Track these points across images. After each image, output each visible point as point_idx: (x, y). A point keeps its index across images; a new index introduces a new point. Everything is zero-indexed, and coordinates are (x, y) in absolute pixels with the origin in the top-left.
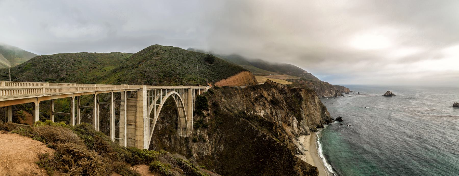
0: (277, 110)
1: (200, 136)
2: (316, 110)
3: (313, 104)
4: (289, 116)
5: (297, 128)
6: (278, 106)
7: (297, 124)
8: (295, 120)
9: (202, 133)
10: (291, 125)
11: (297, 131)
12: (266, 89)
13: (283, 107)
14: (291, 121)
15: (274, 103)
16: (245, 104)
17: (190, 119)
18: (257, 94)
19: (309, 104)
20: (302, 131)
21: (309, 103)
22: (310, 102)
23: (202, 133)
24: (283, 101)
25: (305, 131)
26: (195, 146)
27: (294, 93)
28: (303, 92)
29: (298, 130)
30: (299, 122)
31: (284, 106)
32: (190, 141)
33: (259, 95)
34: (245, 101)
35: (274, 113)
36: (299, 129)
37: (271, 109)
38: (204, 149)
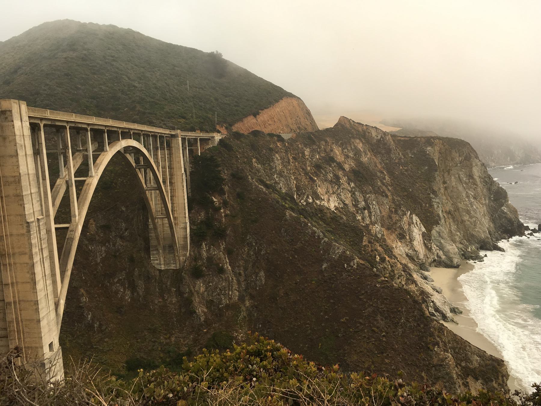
0: (368, 196)
1: (210, 259)
2: (475, 198)
3: (467, 181)
4: (400, 212)
5: (423, 247)
7: (424, 235)
9: (214, 252)
10: (408, 238)
11: (425, 255)
13: (384, 187)
14: (406, 227)
16: (293, 178)
17: (181, 220)
18: (319, 153)
19: (453, 181)
20: (438, 256)
21: (455, 178)
22: (457, 176)
23: (214, 252)
24: (382, 172)
26: (200, 286)
28: (437, 148)
30: (429, 229)
32: (187, 277)
33: (323, 157)
34: (291, 172)
35: (362, 204)
36: (429, 249)
37: (354, 194)
38: (220, 289)
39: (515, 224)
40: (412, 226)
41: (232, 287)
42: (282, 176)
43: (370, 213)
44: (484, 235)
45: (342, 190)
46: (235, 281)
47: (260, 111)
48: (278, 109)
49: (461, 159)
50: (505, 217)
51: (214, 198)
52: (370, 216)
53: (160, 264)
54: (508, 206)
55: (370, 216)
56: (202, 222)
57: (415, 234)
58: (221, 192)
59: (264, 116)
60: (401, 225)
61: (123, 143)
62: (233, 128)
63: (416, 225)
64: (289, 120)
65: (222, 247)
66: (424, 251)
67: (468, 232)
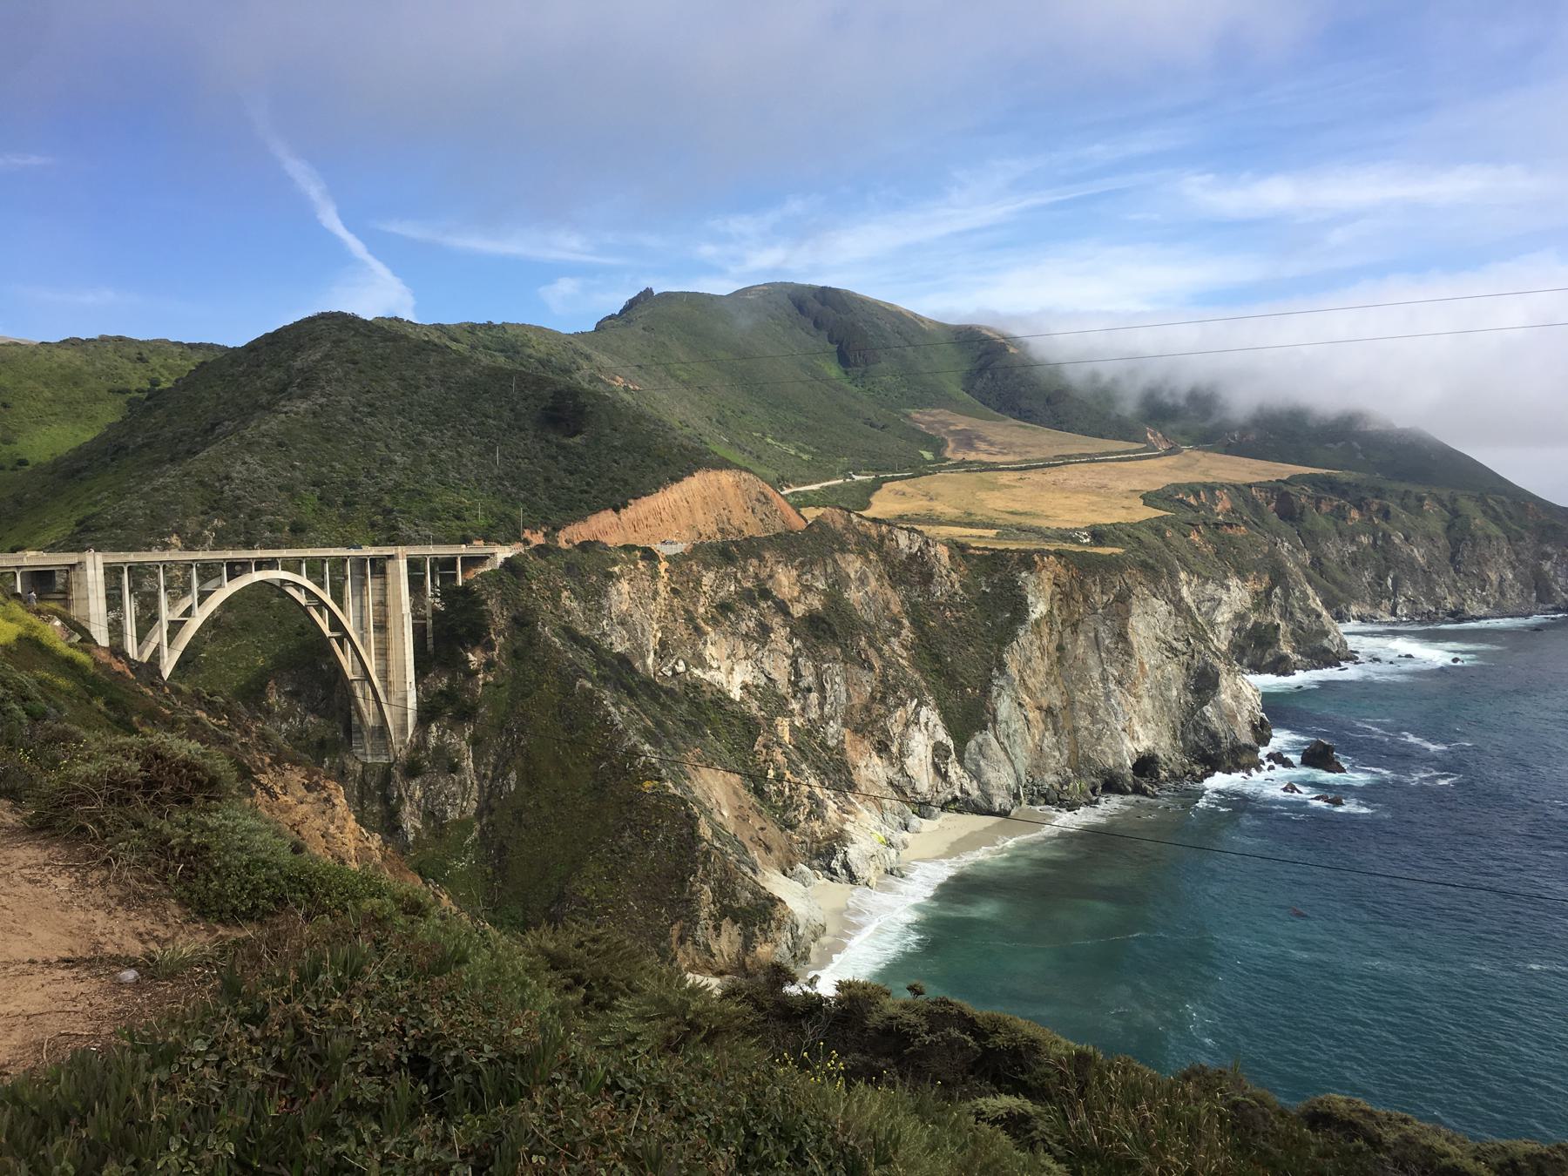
0: (826, 666)
1: (440, 750)
2: (1119, 683)
4: (891, 701)
6: (839, 645)
7: (939, 750)
8: (926, 724)
9: (453, 740)
12: (796, 556)
14: (896, 729)
16: (656, 627)
18: (738, 581)
20: (962, 790)
22: (1092, 635)
23: (453, 740)
27: (989, 576)
29: (939, 780)
35: (809, 679)
36: (944, 776)
38: (446, 796)
39: (1226, 744)
40: (913, 728)
41: (469, 795)
44: (1114, 760)
45: (767, 653)
46: (475, 786)
47: (631, 501)
48: (676, 496)
49: (1105, 598)
50: (1206, 728)
51: (470, 655)
52: (821, 706)
53: (365, 755)
54: (1218, 705)
56: (441, 693)
57: (915, 744)
58: (489, 646)
59: (640, 509)
60: (885, 724)
61: (257, 576)
62: (561, 533)
63: (923, 728)
64: (700, 516)
65: (467, 734)
66: (931, 778)
67: (1081, 752)
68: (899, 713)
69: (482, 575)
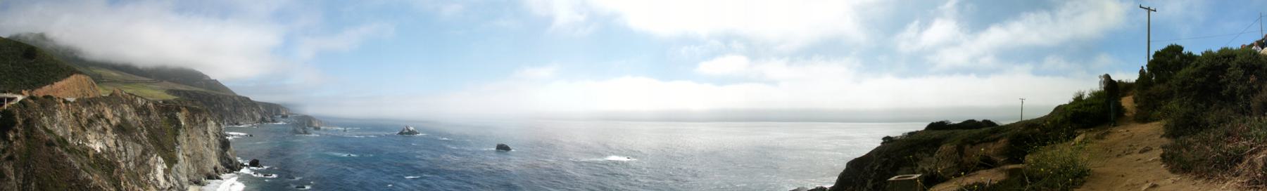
4: (149, 155)
7: (165, 170)
14: (152, 164)
15: (123, 129)
20: (174, 184)
25: (179, 183)
31: (142, 137)
35: (121, 148)
40: (157, 165)
42: (61, 125)
43: (126, 153)
55: (126, 157)
68: (152, 159)
69: (12, 105)
